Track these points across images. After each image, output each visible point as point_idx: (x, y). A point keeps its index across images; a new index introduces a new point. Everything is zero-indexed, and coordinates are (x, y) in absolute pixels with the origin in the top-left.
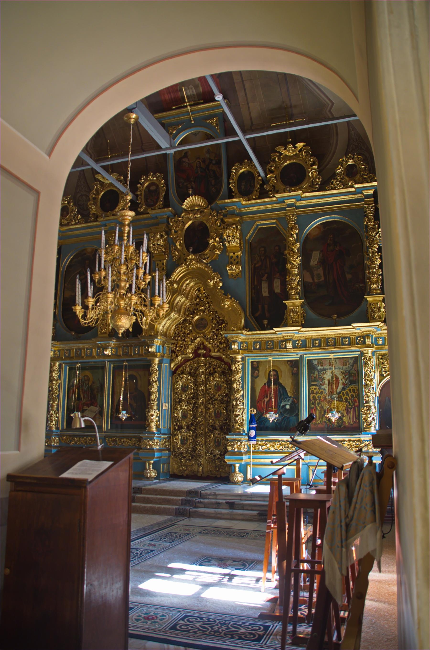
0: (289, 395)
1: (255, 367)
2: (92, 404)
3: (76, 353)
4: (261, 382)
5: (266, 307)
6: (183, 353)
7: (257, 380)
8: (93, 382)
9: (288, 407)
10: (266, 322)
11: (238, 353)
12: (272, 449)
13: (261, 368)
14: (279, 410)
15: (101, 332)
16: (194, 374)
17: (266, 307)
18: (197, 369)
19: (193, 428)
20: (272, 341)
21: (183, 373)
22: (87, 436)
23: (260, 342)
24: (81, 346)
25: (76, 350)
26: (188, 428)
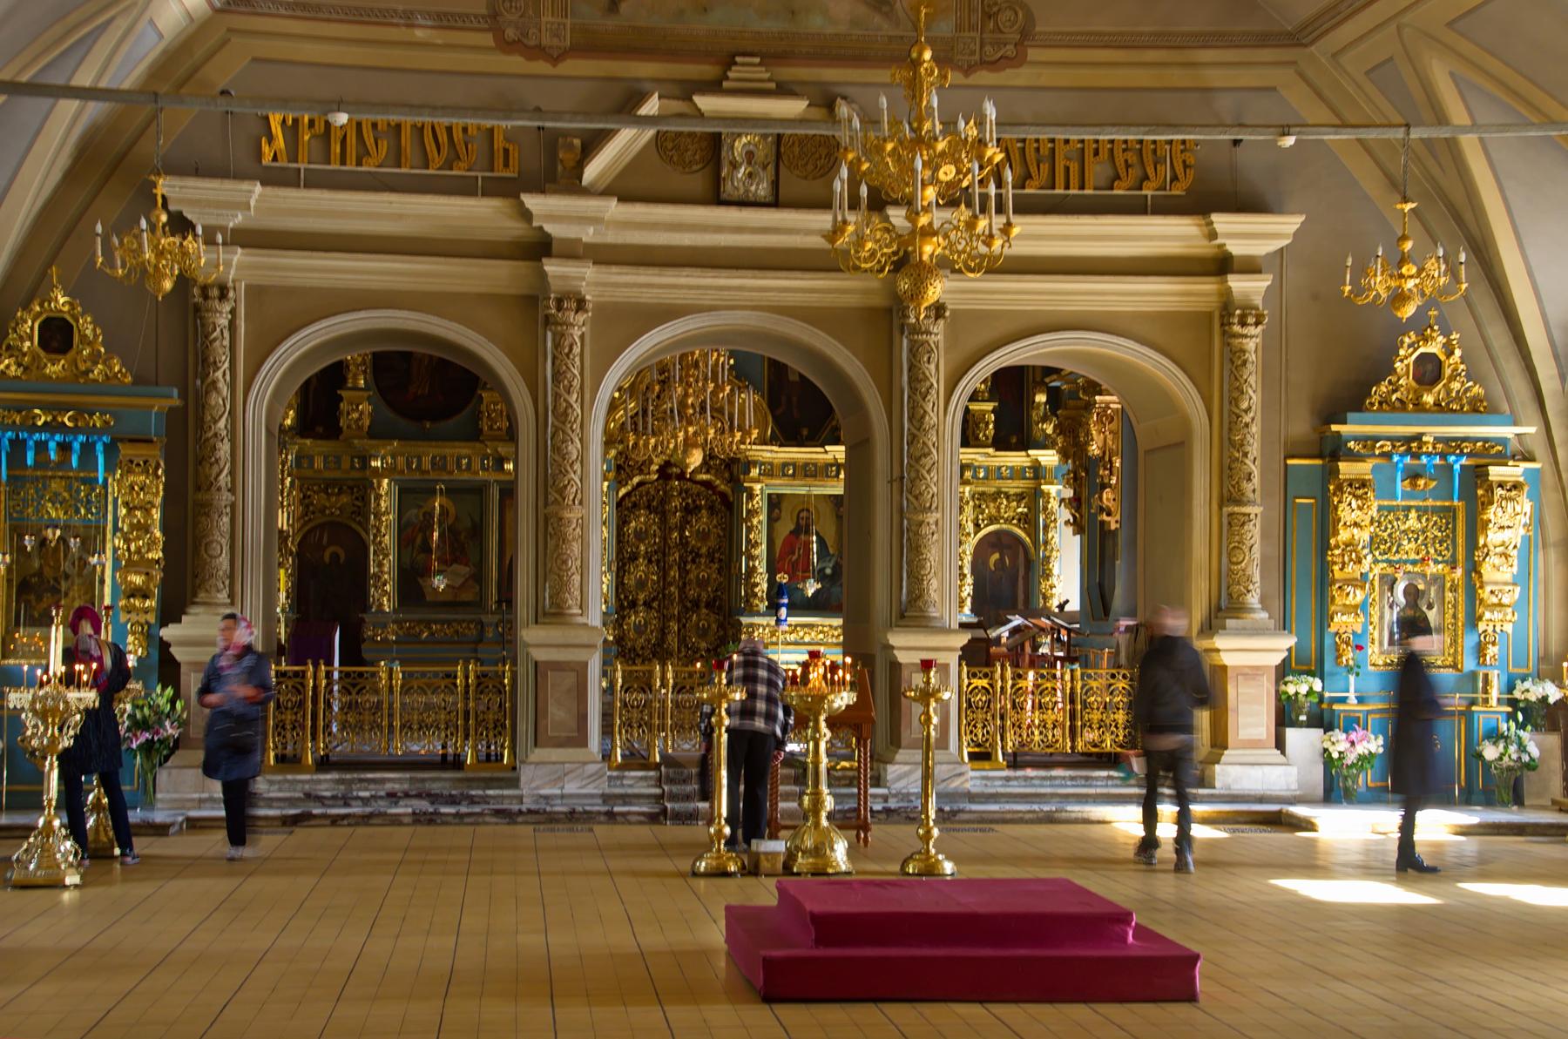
0: (831, 551)
1: (775, 502)
2: (455, 560)
3: (433, 464)
4: (785, 527)
5: (795, 399)
6: (641, 472)
7: (778, 525)
8: (456, 517)
9: (828, 571)
10: (805, 432)
11: (758, 481)
12: (807, 639)
13: (784, 505)
14: (821, 576)
15: (491, 428)
16: (658, 508)
17: (795, 399)
18: (663, 502)
19: (655, 604)
20: (815, 465)
21: (635, 505)
22: (460, 622)
23: (794, 465)
24: (448, 451)
25: (434, 458)
26: (645, 604)
